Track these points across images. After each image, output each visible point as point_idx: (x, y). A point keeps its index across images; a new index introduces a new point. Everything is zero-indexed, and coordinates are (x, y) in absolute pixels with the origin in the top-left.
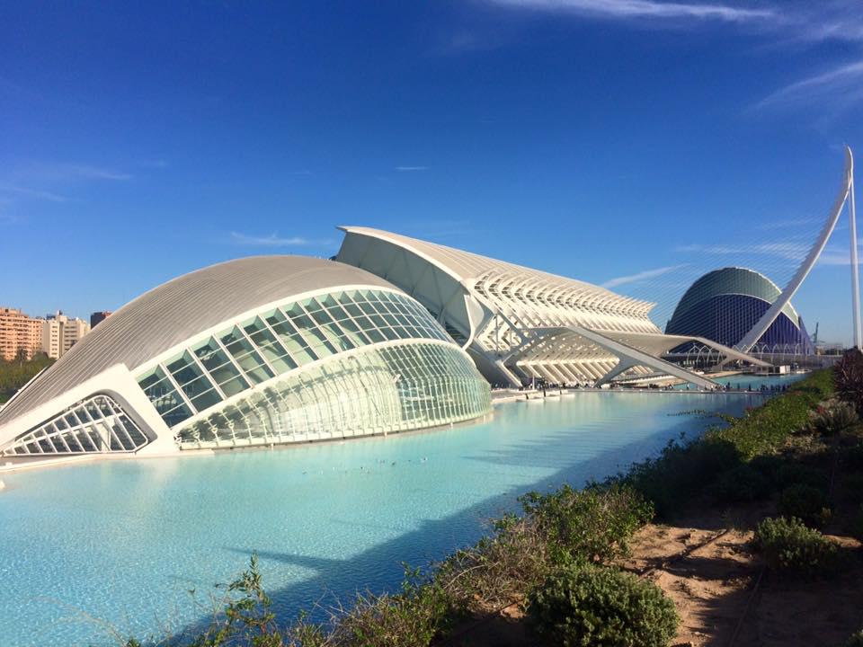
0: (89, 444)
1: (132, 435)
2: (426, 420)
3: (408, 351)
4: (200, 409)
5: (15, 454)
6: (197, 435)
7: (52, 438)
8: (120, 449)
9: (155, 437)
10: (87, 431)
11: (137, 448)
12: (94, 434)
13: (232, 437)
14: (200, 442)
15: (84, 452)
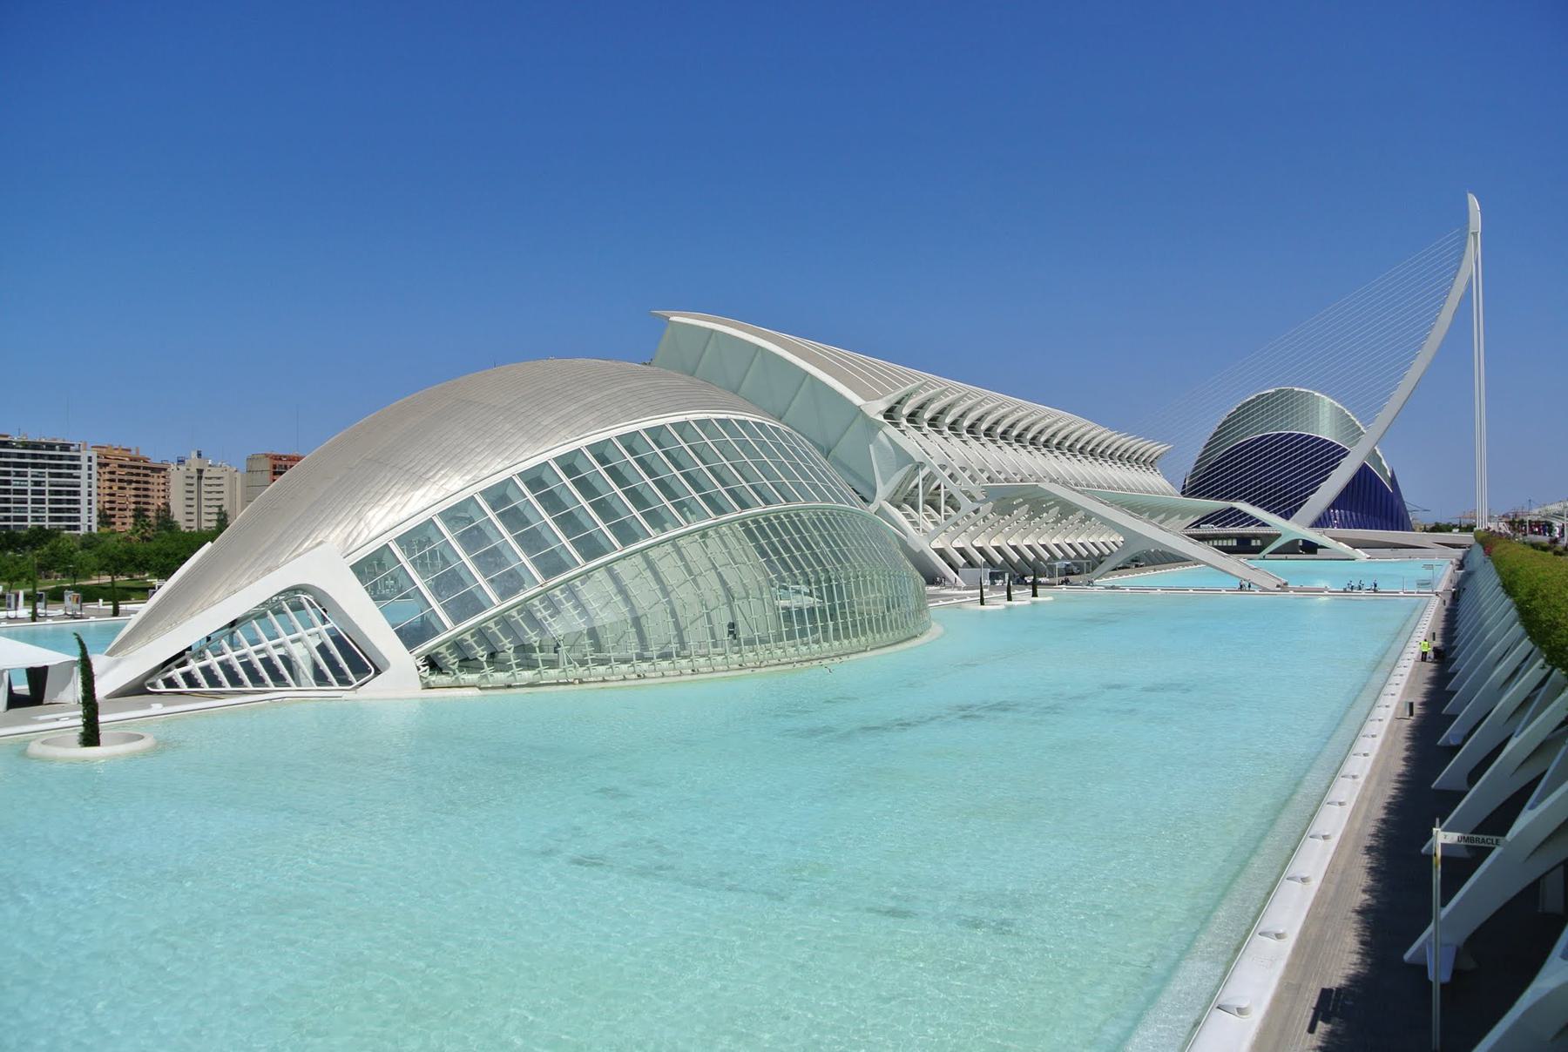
0: (277, 672)
1: (349, 661)
2: (817, 642)
3: (793, 522)
5: (163, 688)
6: (452, 660)
7: (221, 663)
8: (331, 684)
10: (275, 654)
12: (287, 660)
13: (510, 667)
15: (272, 687)
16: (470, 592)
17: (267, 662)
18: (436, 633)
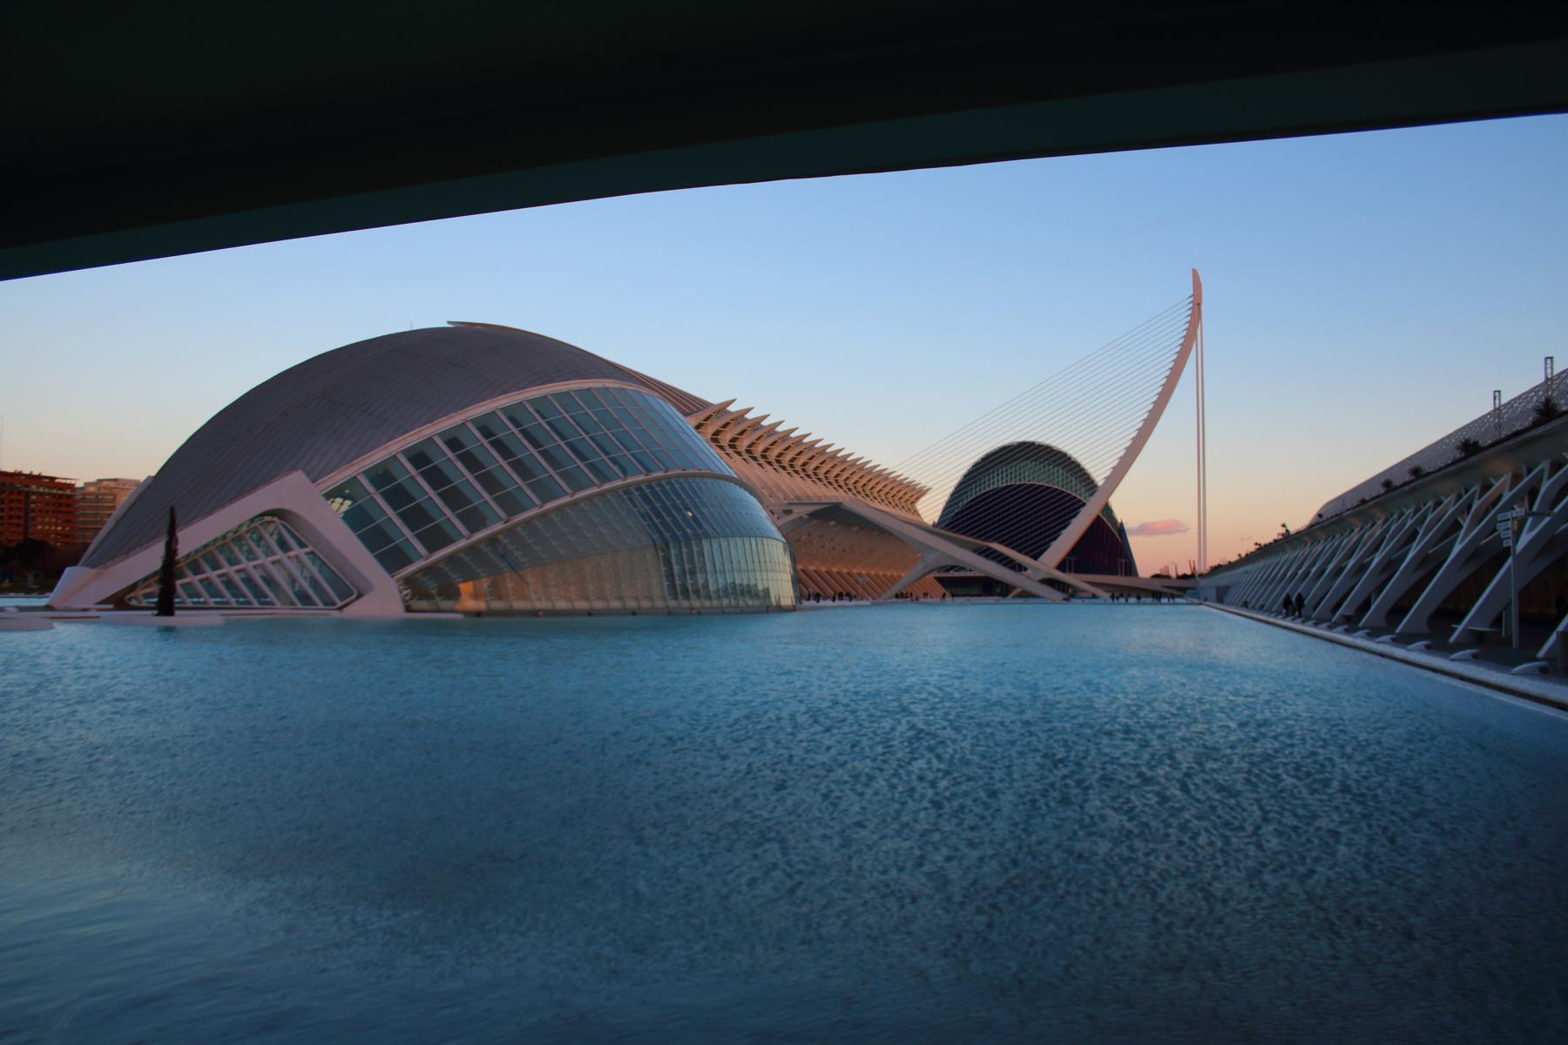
4: (432, 549)
6: (432, 587)
9: (371, 588)
10: (256, 576)
11: (340, 604)
12: (269, 580)
14: (438, 599)
15: (256, 605)
16: (437, 526)
17: (249, 581)
18: (410, 562)
